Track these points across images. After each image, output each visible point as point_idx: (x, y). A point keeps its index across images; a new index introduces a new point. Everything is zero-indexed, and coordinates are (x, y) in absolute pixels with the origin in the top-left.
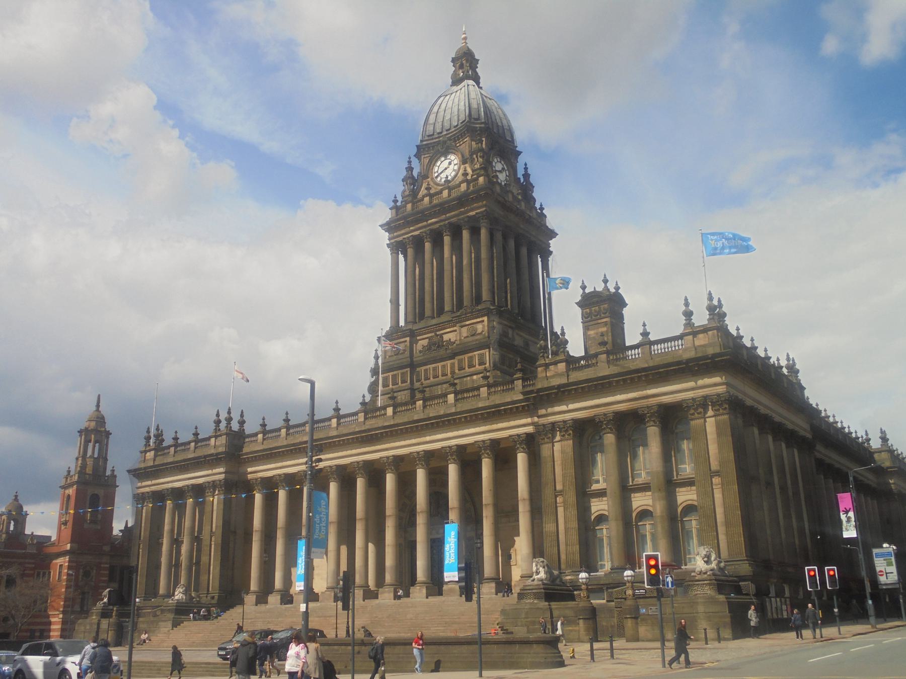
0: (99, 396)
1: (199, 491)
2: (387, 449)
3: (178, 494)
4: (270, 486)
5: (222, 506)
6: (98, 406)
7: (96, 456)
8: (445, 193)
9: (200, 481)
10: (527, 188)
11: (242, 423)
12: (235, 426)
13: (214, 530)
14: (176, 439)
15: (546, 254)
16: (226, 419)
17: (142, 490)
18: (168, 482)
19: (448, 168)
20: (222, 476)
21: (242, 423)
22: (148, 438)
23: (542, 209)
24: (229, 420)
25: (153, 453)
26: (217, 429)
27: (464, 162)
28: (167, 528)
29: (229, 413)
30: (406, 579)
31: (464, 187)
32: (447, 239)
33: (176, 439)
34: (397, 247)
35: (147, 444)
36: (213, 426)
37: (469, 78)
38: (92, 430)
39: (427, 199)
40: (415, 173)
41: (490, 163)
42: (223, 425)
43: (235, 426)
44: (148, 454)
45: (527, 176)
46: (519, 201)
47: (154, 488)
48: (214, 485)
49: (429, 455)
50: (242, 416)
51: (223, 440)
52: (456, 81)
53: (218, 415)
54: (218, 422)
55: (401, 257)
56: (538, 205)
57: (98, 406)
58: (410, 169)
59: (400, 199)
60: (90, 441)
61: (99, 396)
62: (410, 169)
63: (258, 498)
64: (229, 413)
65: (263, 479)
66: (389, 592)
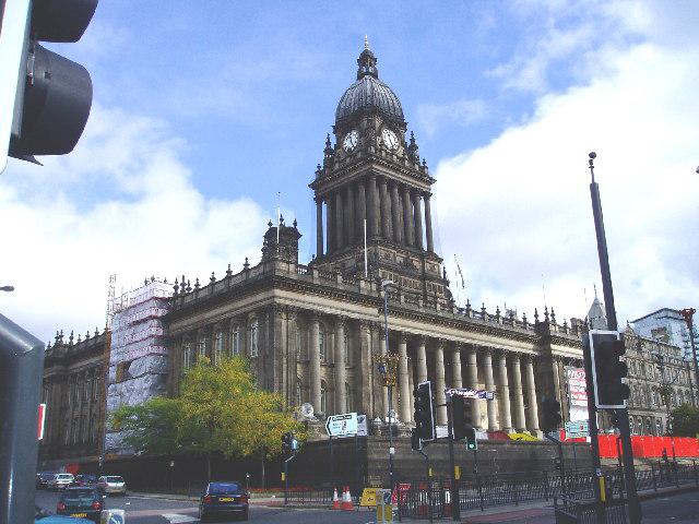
8: (348, 160)
10: (411, 149)
15: (427, 196)
19: (352, 140)
23: (424, 163)
27: (360, 136)
31: (359, 155)
32: (350, 192)
34: (318, 200)
37: (367, 73)
39: (337, 165)
40: (333, 147)
41: (380, 134)
45: (413, 140)
46: (403, 160)
52: (360, 76)
55: (324, 206)
56: (421, 161)
58: (328, 143)
59: (322, 165)
62: (328, 143)
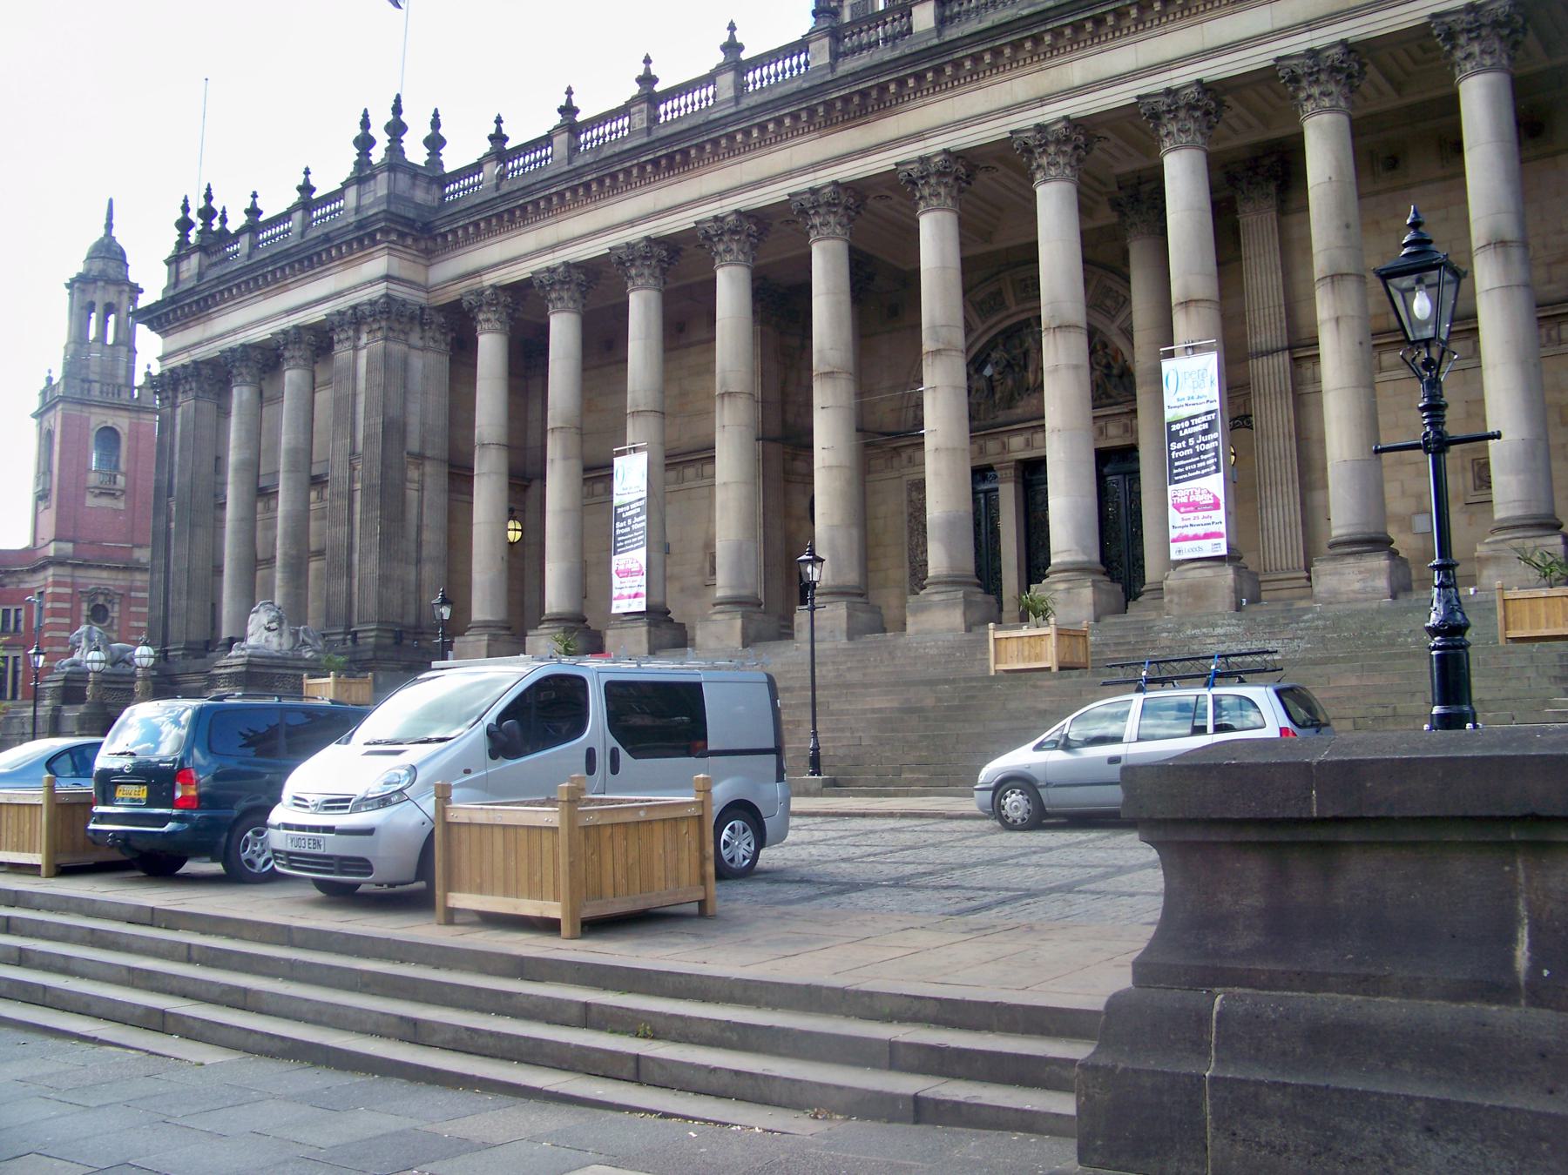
0: (111, 201)
1: (318, 342)
2: (918, 136)
3: (265, 360)
4: (523, 308)
5: (379, 378)
6: (109, 226)
7: (110, 340)
9: (317, 314)
11: (435, 143)
12: (416, 153)
13: (360, 448)
14: (254, 212)
16: (388, 128)
17: (175, 362)
18: (234, 331)
20: (379, 290)
21: (435, 143)
22: (184, 225)
24: (397, 129)
25: (195, 259)
26: (363, 162)
28: (233, 457)
29: (397, 109)
30: (1004, 562)
33: (254, 212)
35: (183, 242)
36: (353, 154)
38: (95, 280)
42: (377, 155)
43: (416, 153)
44: (184, 266)
47: (200, 354)
48: (356, 319)
49: (1083, 135)
50: (436, 123)
51: (380, 187)
53: (365, 124)
54: (364, 143)
57: (109, 226)
60: (91, 307)
61: (111, 201)
63: (490, 348)
64: (397, 109)
65: (499, 289)
66: (948, 605)
